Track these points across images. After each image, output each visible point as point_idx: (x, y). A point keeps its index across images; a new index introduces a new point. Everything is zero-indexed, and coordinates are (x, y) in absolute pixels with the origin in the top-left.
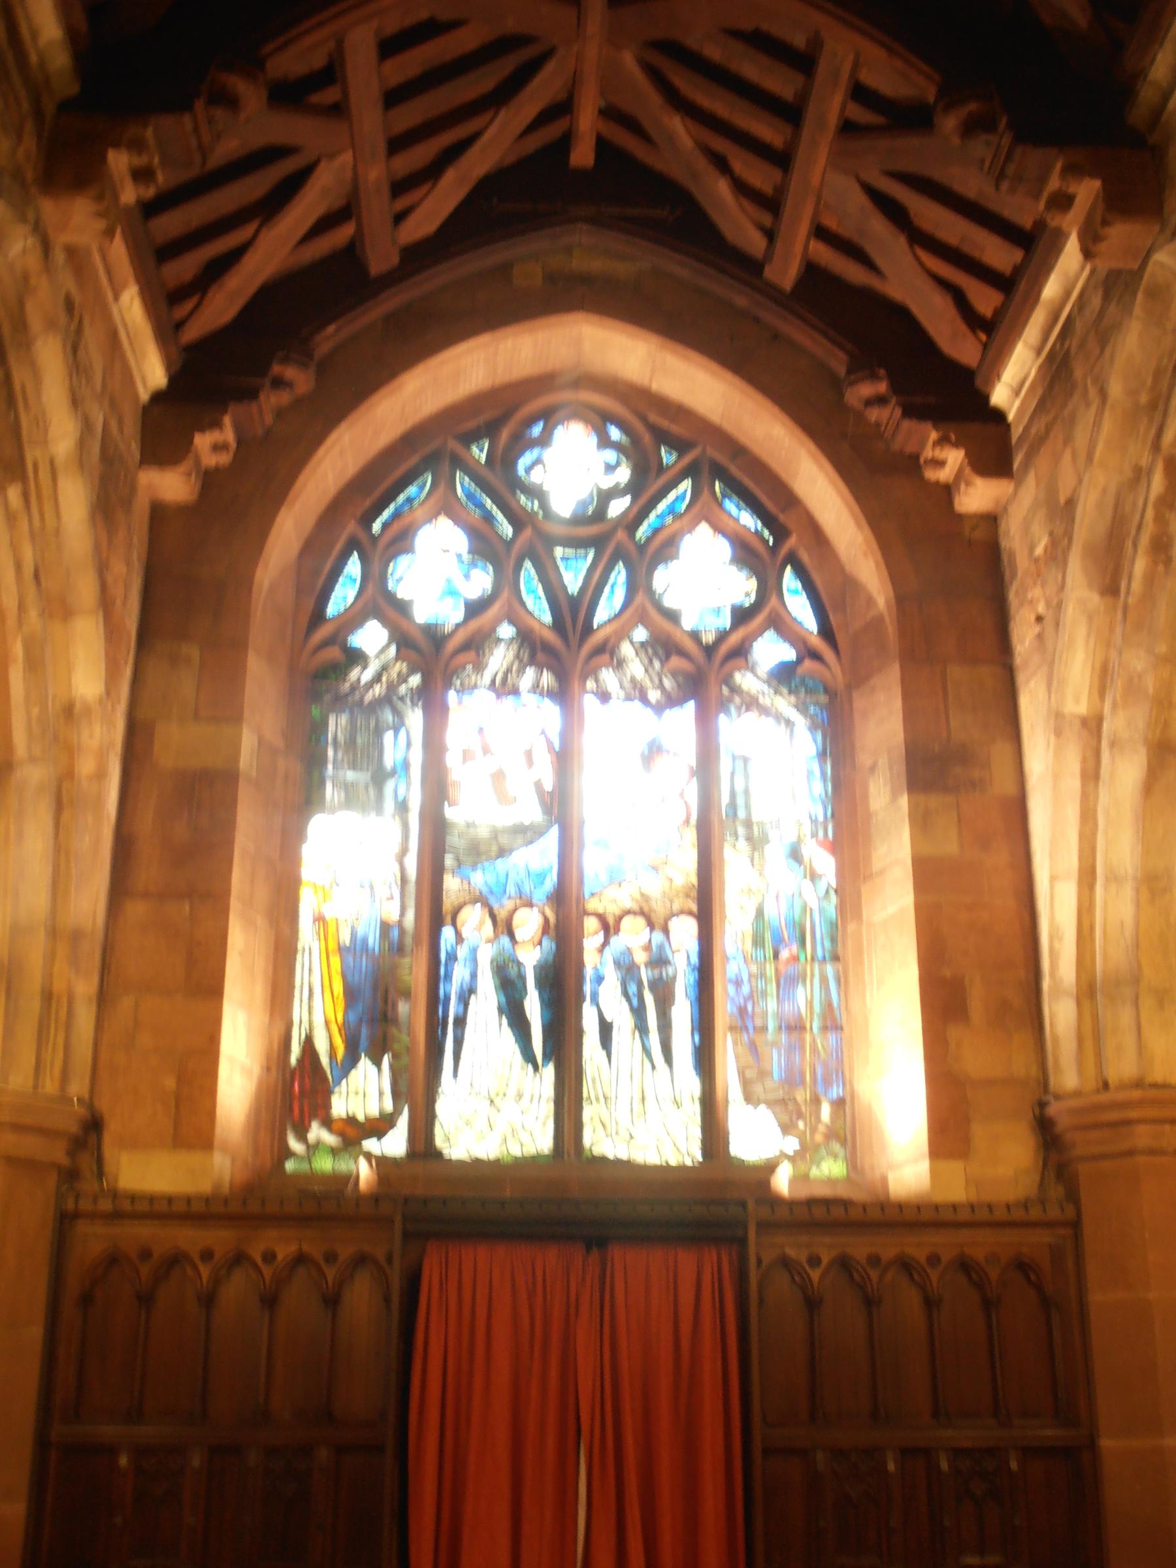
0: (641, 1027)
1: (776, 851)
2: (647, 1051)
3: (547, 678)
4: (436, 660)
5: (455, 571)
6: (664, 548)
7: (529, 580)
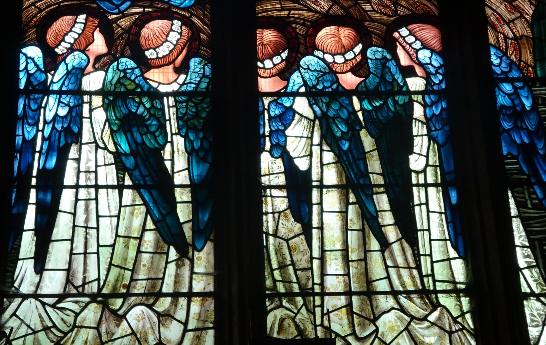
0: (355, 184)
2: (370, 221)
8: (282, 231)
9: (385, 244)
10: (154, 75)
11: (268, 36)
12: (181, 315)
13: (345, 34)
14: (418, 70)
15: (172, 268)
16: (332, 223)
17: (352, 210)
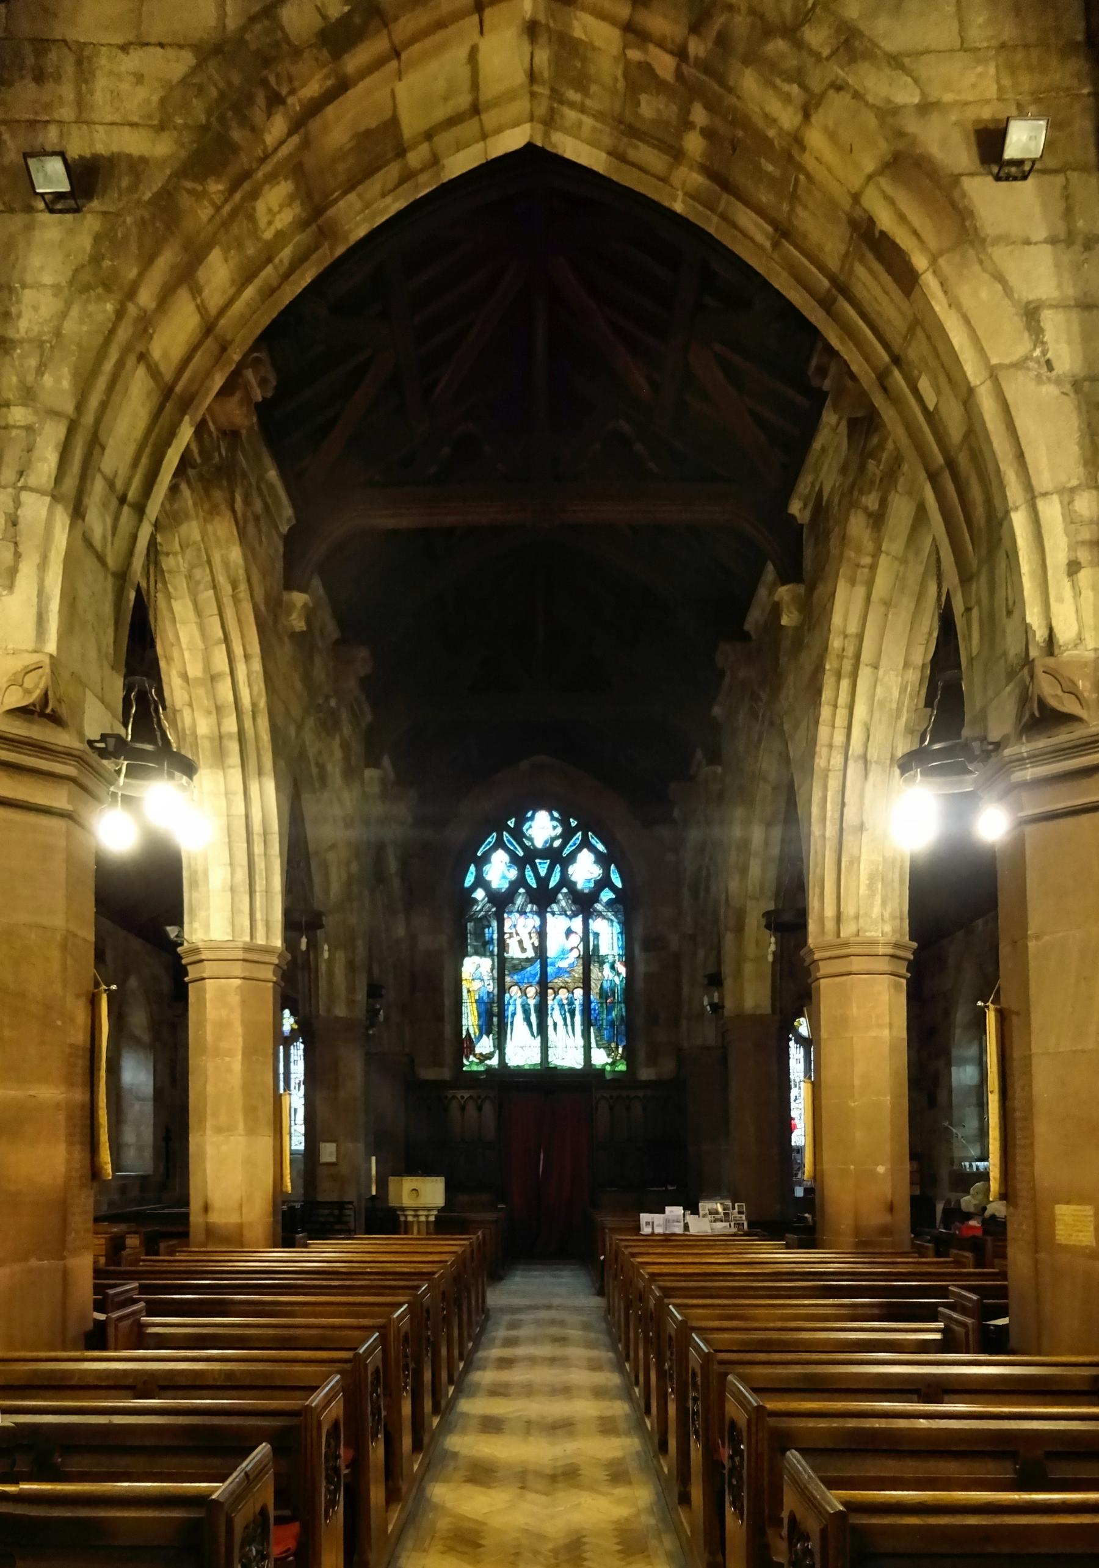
0: (566, 1024)
1: (607, 967)
3: (535, 908)
4: (501, 902)
5: (505, 869)
6: (572, 858)
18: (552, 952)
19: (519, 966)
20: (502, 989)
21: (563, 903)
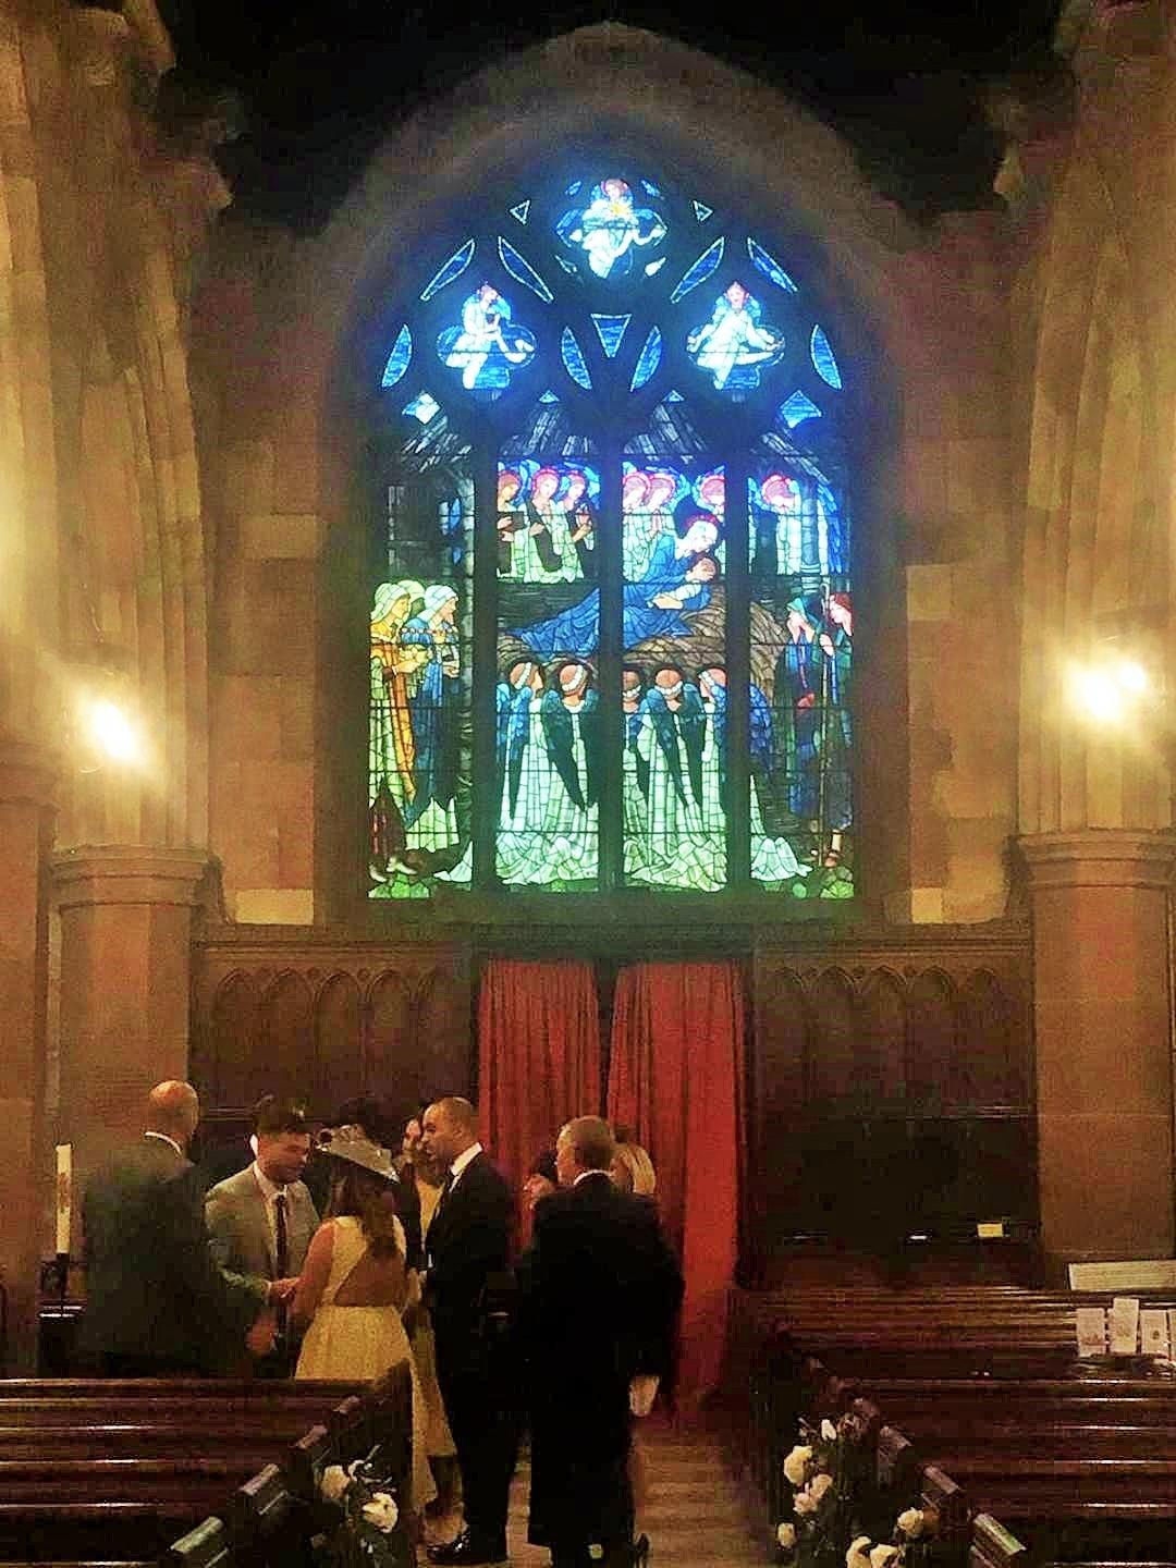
0: (673, 769)
2: (679, 789)
7: (570, 350)
8: (633, 798)
9: (686, 805)
10: (567, 701)
11: (630, 676)
12: (581, 842)
13: (674, 674)
14: (711, 699)
15: (577, 816)
16: (660, 793)
17: (671, 785)
18: (636, 564)
19: (537, 606)
20: (489, 672)
21: (671, 433)
